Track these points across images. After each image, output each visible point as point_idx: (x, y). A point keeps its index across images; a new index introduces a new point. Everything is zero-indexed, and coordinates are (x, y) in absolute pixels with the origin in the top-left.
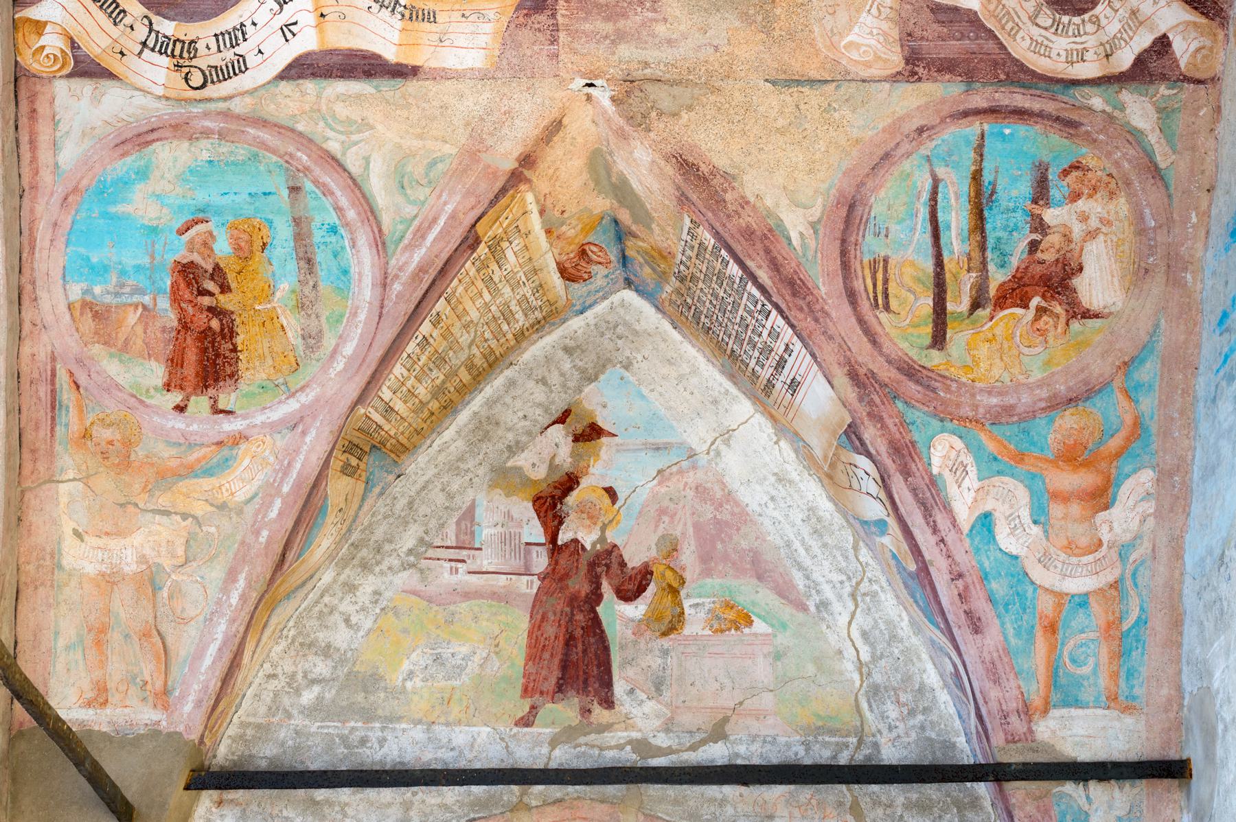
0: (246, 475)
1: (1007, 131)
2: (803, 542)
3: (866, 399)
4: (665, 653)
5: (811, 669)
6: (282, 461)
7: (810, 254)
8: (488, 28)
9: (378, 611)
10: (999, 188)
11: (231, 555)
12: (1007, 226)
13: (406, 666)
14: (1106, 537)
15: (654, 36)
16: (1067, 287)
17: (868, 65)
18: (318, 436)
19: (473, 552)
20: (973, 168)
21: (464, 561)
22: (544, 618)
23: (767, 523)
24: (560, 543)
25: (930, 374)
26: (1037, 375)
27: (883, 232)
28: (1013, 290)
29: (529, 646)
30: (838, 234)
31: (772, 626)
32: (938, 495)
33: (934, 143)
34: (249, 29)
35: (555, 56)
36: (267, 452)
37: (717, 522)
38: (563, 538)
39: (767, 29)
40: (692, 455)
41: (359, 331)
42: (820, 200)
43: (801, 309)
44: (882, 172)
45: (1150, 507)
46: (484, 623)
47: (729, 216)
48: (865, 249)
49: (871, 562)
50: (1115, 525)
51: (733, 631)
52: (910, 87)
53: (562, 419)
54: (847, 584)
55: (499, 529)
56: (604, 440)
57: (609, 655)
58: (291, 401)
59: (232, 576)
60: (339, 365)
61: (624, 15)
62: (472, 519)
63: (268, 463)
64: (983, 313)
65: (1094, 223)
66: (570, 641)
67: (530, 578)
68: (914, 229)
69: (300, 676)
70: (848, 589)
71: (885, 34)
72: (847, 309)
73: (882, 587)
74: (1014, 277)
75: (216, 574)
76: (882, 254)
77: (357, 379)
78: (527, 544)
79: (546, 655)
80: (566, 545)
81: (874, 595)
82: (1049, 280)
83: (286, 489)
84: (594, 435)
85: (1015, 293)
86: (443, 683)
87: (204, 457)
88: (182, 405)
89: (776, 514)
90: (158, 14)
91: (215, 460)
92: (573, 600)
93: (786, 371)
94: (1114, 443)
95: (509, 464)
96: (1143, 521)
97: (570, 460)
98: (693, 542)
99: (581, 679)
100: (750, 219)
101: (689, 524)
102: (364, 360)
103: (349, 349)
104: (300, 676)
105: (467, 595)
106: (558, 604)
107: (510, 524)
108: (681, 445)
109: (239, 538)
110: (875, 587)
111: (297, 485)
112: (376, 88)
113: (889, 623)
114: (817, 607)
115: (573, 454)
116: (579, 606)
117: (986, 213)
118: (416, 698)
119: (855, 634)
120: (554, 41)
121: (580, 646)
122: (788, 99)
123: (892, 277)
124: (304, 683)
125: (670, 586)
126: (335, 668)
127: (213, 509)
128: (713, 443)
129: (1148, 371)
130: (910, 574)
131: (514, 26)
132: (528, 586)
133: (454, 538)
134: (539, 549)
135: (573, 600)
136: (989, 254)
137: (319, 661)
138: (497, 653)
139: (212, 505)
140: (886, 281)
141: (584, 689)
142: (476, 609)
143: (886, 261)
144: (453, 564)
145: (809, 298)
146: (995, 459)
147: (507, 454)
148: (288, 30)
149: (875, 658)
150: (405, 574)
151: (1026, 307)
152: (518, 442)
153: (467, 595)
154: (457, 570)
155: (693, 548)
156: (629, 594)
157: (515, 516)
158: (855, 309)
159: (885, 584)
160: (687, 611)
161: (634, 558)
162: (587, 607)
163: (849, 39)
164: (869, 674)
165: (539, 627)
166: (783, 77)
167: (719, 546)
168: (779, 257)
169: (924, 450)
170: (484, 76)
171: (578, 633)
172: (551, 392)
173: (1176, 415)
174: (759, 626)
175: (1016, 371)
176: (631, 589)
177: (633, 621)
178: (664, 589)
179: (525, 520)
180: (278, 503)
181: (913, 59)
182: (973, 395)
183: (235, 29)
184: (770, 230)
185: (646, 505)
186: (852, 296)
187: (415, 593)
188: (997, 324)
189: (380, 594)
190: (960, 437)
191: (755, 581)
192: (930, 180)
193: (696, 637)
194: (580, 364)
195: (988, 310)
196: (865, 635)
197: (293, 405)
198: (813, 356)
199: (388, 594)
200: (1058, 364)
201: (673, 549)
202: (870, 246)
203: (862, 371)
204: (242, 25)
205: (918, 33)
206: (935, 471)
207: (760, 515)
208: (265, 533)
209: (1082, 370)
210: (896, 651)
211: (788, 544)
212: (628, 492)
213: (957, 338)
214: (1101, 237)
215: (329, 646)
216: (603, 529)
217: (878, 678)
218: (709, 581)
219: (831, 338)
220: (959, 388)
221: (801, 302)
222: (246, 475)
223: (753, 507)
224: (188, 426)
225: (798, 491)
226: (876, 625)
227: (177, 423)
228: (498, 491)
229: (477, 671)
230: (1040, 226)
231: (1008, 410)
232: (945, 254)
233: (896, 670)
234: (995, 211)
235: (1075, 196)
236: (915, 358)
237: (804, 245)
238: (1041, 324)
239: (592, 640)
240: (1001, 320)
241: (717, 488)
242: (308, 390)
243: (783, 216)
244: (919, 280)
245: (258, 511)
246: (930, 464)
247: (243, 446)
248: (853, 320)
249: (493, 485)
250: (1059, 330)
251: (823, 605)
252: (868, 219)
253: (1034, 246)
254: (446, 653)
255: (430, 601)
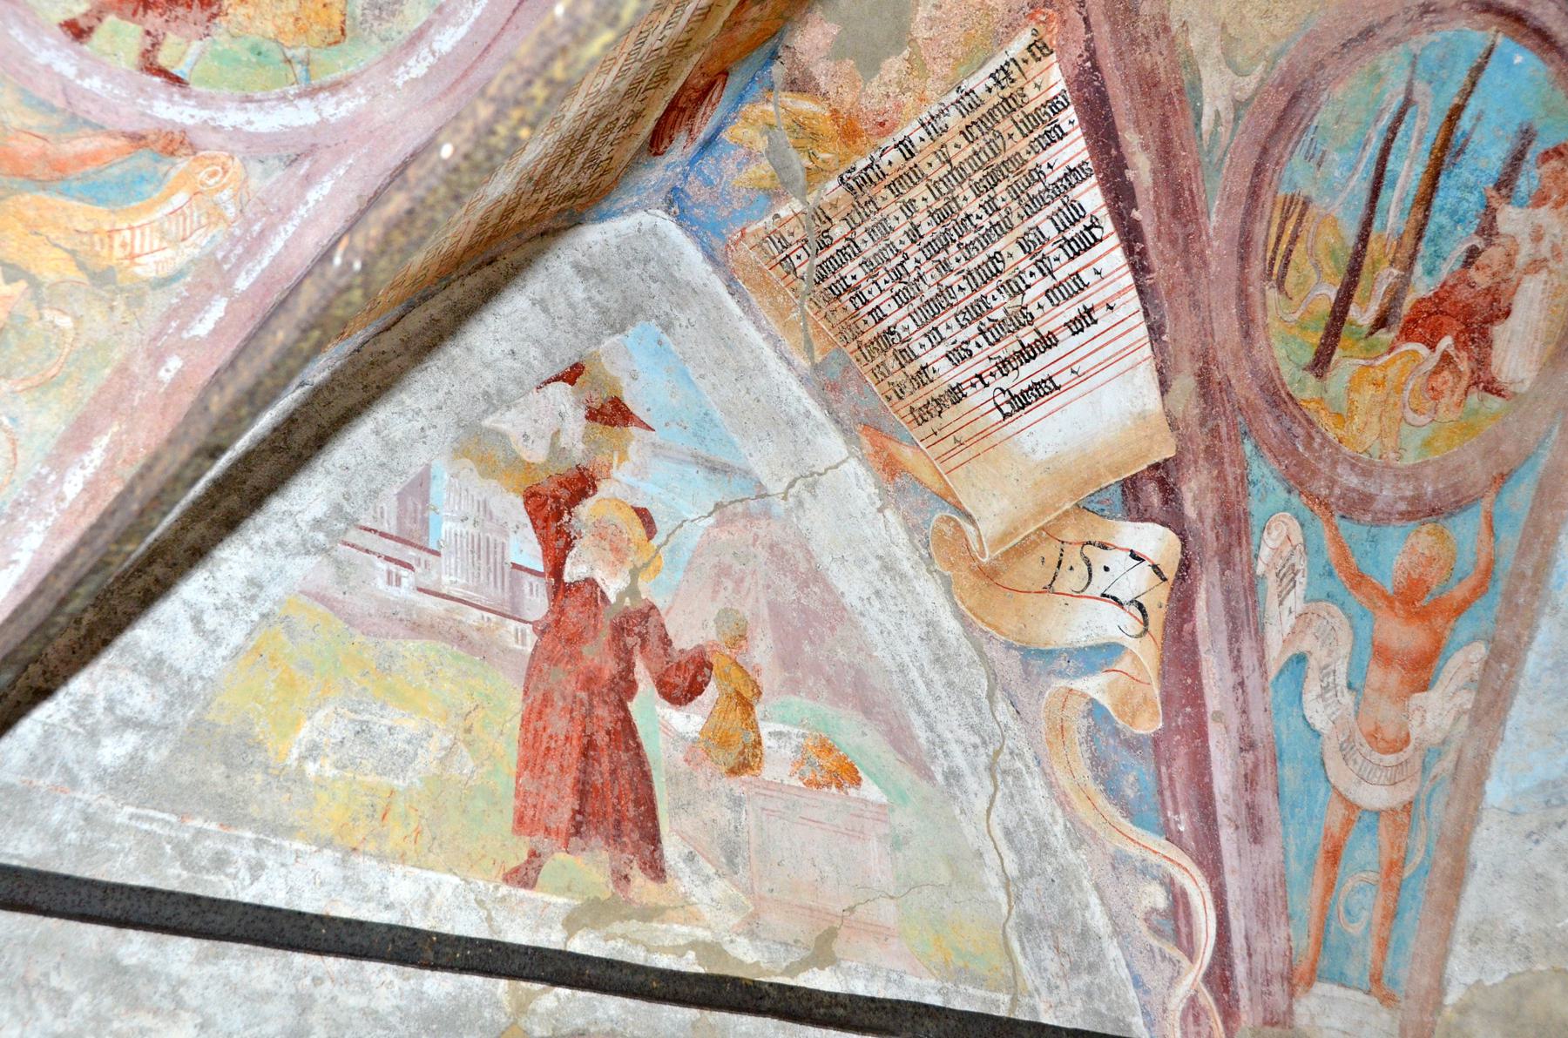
0: (173, 228)
1: (1518, 59)
2: (921, 668)
3: (1210, 424)
4: (737, 803)
5: (943, 874)
6: (249, 224)
7: (1218, 153)
9: (255, 616)
10: (1471, 146)
11: (90, 389)
12: (1455, 212)
13: (305, 733)
14: (1415, 732)
16: (1484, 334)
18: (331, 197)
19: (424, 556)
20: (1456, 100)
21: (409, 567)
22: (547, 700)
23: (873, 630)
24: (567, 579)
25: (1296, 412)
26: (1410, 459)
27: (1318, 155)
28: (1430, 315)
29: (524, 744)
30: (1262, 135)
31: (886, 791)
32: (1254, 609)
33: (1433, 37)
36: (225, 195)
37: (804, 610)
38: (573, 571)
40: (763, 495)
41: (477, 12)
42: (1260, 68)
43: (1173, 242)
44: (1352, 56)
45: (1467, 699)
46: (447, 685)
47: (1133, 41)
48: (1286, 175)
49: (1011, 724)
50: (1429, 716)
51: (834, 789)
53: (572, 375)
54: (982, 750)
55: (468, 528)
56: (633, 430)
57: (651, 788)
58: (304, 103)
59: (78, 436)
60: (418, 66)
62: (426, 500)
63: (221, 217)
64: (1384, 336)
65: (1545, 249)
66: (588, 749)
67: (521, 625)
68: (1354, 168)
69: (99, 706)
70: (983, 760)
72: (1234, 267)
73: (1028, 767)
74: (1436, 294)
75: (47, 421)
76: (1304, 192)
77: (441, 107)
78: (515, 566)
79: (552, 766)
80: (576, 586)
81: (1018, 776)
82: (1471, 315)
83: (242, 283)
84: (618, 417)
85: (1424, 323)
86: (372, 779)
87: (96, 156)
88: (83, 24)
89: (882, 617)
91: (116, 171)
92: (590, 681)
93: (1026, 370)
94: (1459, 592)
95: (487, 422)
96: (1456, 720)
97: (581, 446)
98: (769, 633)
99: (611, 820)
100: (1159, 59)
101: (763, 601)
102: (465, 75)
103: (447, 40)
104: (99, 706)
105: (418, 627)
106: (564, 682)
107: (487, 524)
108: (747, 473)
109: (117, 355)
110: (1019, 764)
111: (265, 282)
113: (1038, 822)
114: (946, 778)
115: (586, 438)
116: (601, 694)
117: (1442, 178)
118: (324, 797)
119: (998, 833)
121: (605, 760)
123: (1303, 234)
124: (107, 721)
125: (738, 693)
126: (170, 705)
127: (82, 277)
128: (791, 485)
129: (1521, 494)
130: (1133, 745)
132: (520, 640)
133: (394, 522)
134: (532, 578)
135: (590, 681)
136: (1422, 246)
137: (139, 683)
138: (469, 744)
139: (81, 266)
140: (1294, 239)
141: (615, 838)
142: (432, 655)
143: (1306, 204)
144: (393, 567)
145: (1192, 228)
146: (1330, 574)
147: (483, 406)
149: (1025, 875)
150: (309, 562)
151: (1432, 347)
152: (500, 392)
153: (418, 627)
154: (399, 579)
155: (769, 641)
156: (677, 692)
157: (496, 513)
158: (1243, 268)
159: (1032, 764)
160: (767, 742)
161: (689, 632)
162: (613, 697)
164: (1018, 898)
165: (540, 713)
167: (807, 648)
168: (1177, 143)
169: (1257, 530)
171: (601, 739)
172: (555, 327)
173: (1529, 572)
174: (870, 790)
175: (1389, 442)
176: (683, 684)
177: (683, 738)
178: (729, 697)
179: (511, 525)
180: (217, 310)
182: (1334, 463)
184: (1180, 91)
185: (697, 553)
186: (1245, 244)
187: (322, 599)
188: (1393, 361)
189: (261, 587)
190: (1302, 525)
191: (861, 717)
192: (1401, 97)
193: (780, 787)
194: (598, 298)
195: (1393, 335)
196: (1008, 833)
197: (302, 115)
198: (1155, 331)
199: (275, 591)
200: (1436, 451)
201: (740, 638)
202: (1296, 175)
203: (1217, 376)
206: (1260, 569)
207: (862, 614)
208: (174, 363)
209: (1457, 469)
210: (1049, 869)
211: (902, 670)
212: (671, 525)
213: (1345, 364)
214: (1543, 275)
215: (159, 660)
216: (634, 574)
217: (1029, 905)
218: (795, 699)
219: (1196, 305)
220: (1322, 446)
221: (1178, 230)
222: (173, 228)
223: (851, 599)
224: (81, 74)
225: (912, 591)
226: (1021, 824)
227: (61, 59)
228: (468, 462)
229: (434, 768)
230: (1488, 230)
231: (1366, 500)
232: (1376, 224)
233: (1051, 897)
234: (1452, 182)
235: (1540, 199)
236: (1286, 379)
237: (1214, 133)
238: (1437, 382)
239: (624, 757)
240: (1401, 355)
241: (800, 555)
242: (344, 94)
243: (1205, 74)
244: (1332, 253)
245: (172, 313)
246: (1256, 556)
247: (182, 164)
248: (1233, 287)
249: (460, 452)
250: (1455, 398)
251: (953, 775)
252: (1307, 127)
253: (1473, 253)
254: (380, 725)
255: (348, 621)
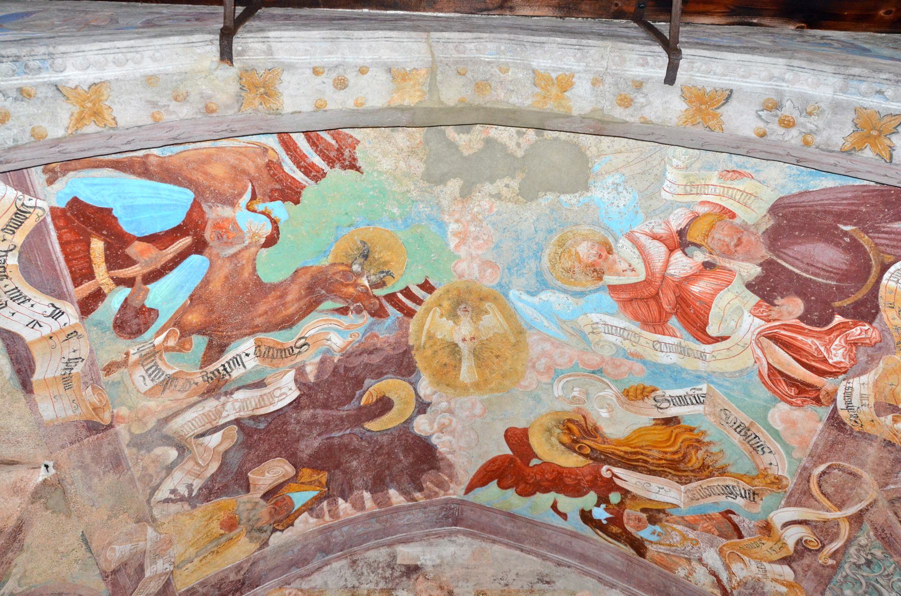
8: (70, 413)
15: (91, 479)
17: (106, 560)
34: (28, 304)
35: (63, 447)
39: (109, 518)
52: (101, 580)
61: (97, 463)
71: (123, 557)
90: (20, 253)
112: (11, 378)
120: (72, 443)
122: (76, 544)
131: (76, 424)
148: (35, 324)
163: (117, 547)
166: (87, 536)
170: (40, 424)
181: (114, 572)
183: (25, 297)
204: (29, 300)
205: (127, 566)
